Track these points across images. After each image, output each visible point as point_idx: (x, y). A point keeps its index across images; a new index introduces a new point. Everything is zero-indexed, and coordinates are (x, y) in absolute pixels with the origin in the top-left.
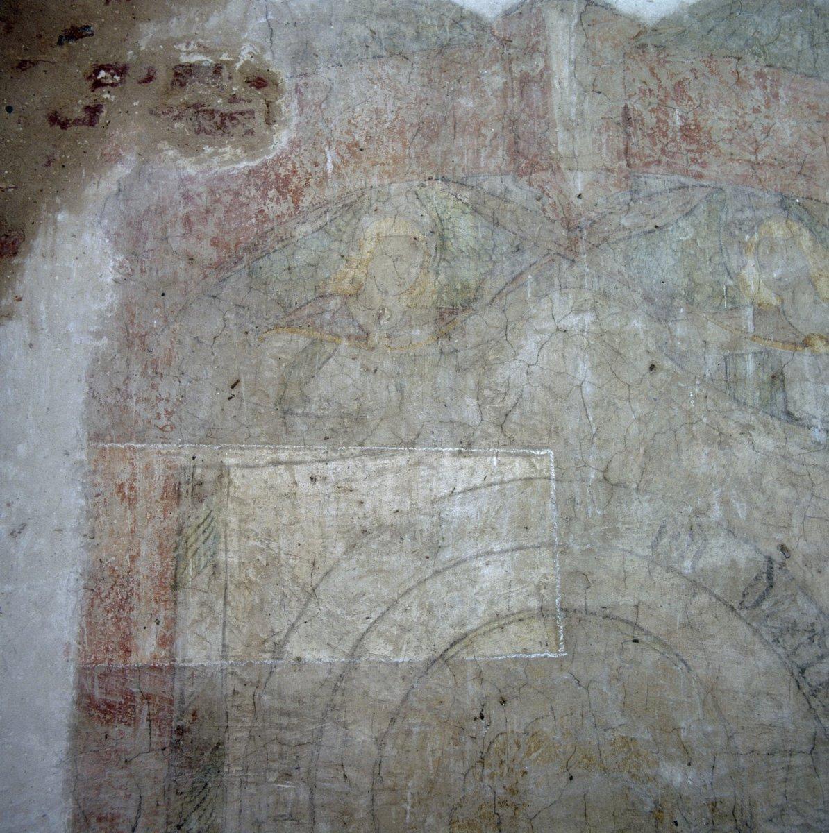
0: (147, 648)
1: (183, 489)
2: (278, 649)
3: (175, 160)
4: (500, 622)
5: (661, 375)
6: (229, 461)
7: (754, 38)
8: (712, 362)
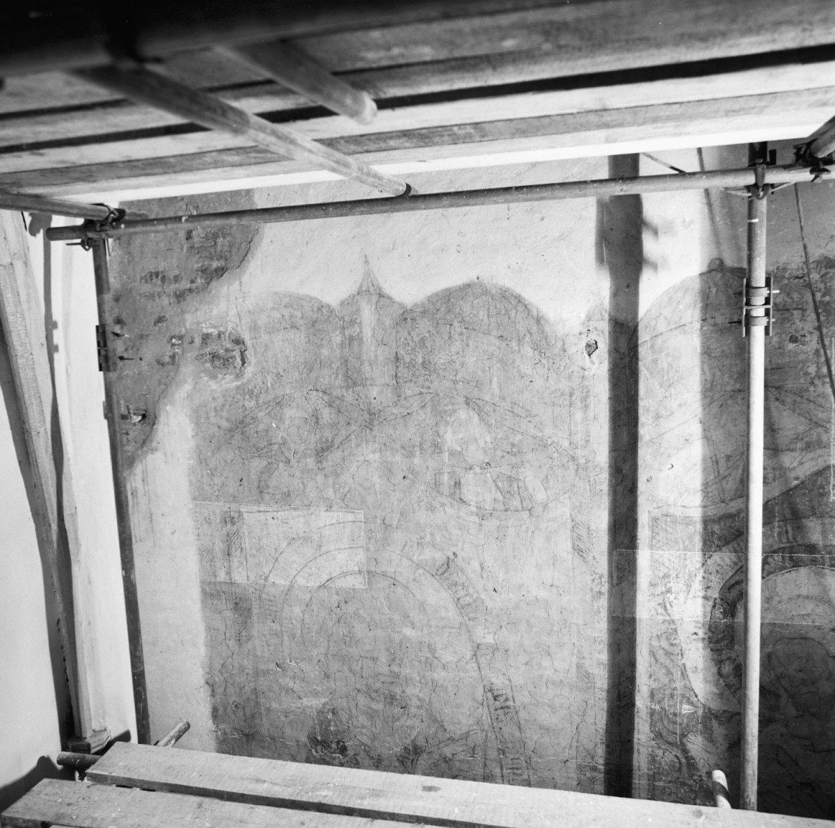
0: (222, 576)
1: (227, 519)
2: (266, 579)
3: (208, 382)
4: (344, 574)
5: (407, 481)
6: (243, 510)
7: (459, 313)
8: (429, 476)
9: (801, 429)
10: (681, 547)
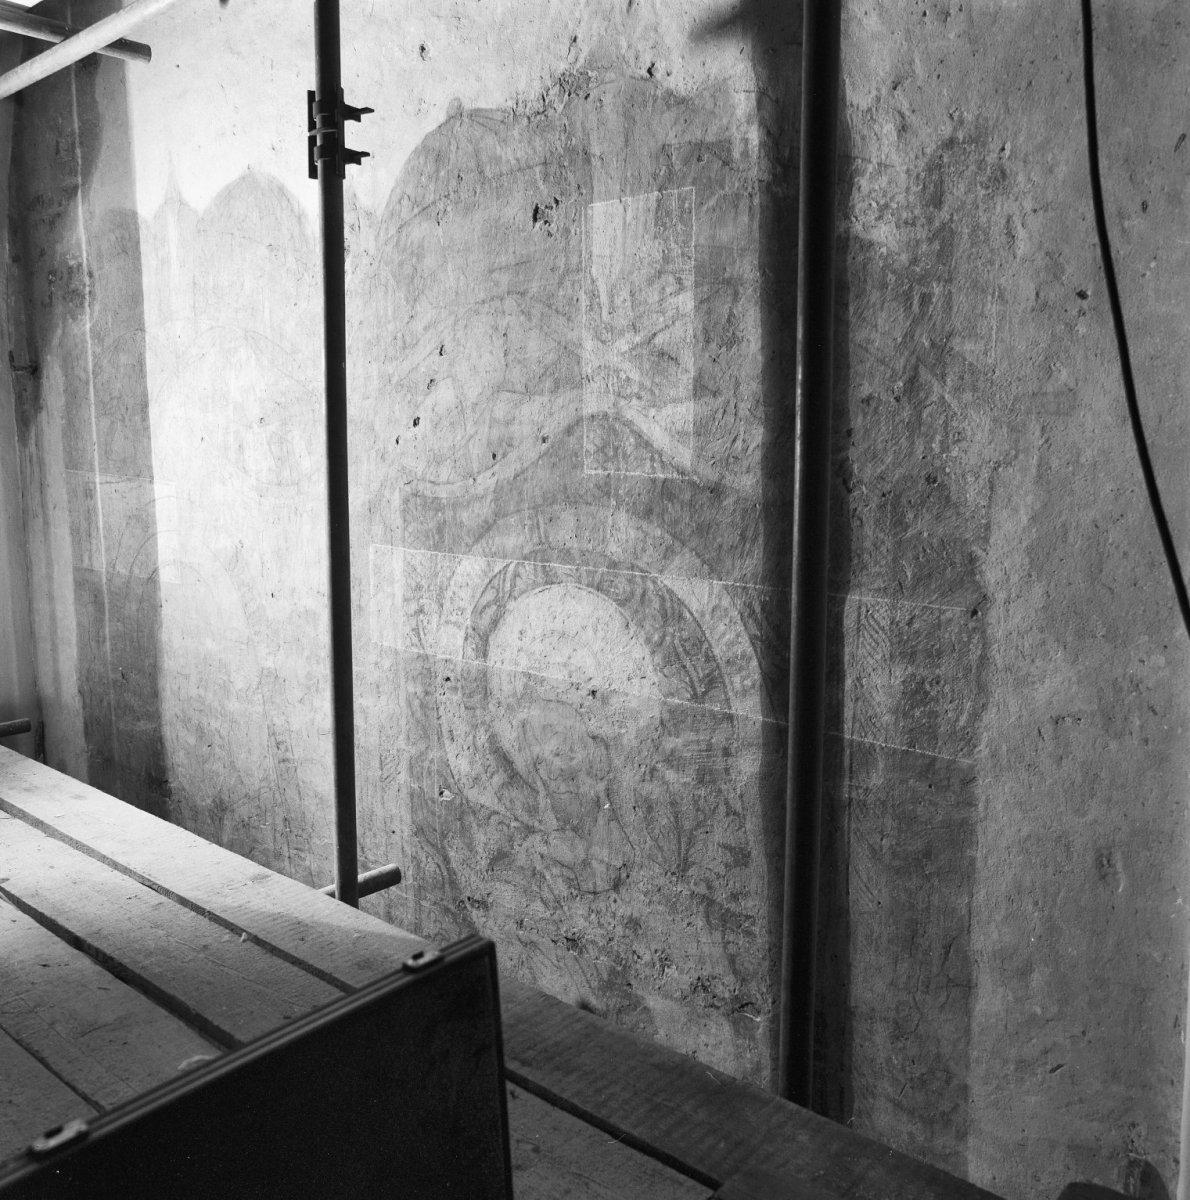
9: (551, 357)
10: (431, 543)
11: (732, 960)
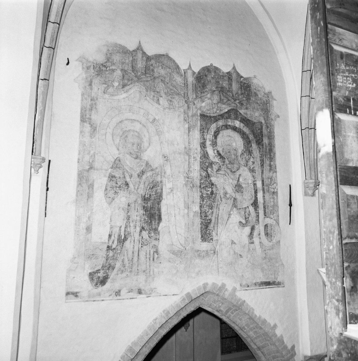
11: (253, 176)
